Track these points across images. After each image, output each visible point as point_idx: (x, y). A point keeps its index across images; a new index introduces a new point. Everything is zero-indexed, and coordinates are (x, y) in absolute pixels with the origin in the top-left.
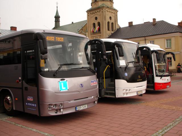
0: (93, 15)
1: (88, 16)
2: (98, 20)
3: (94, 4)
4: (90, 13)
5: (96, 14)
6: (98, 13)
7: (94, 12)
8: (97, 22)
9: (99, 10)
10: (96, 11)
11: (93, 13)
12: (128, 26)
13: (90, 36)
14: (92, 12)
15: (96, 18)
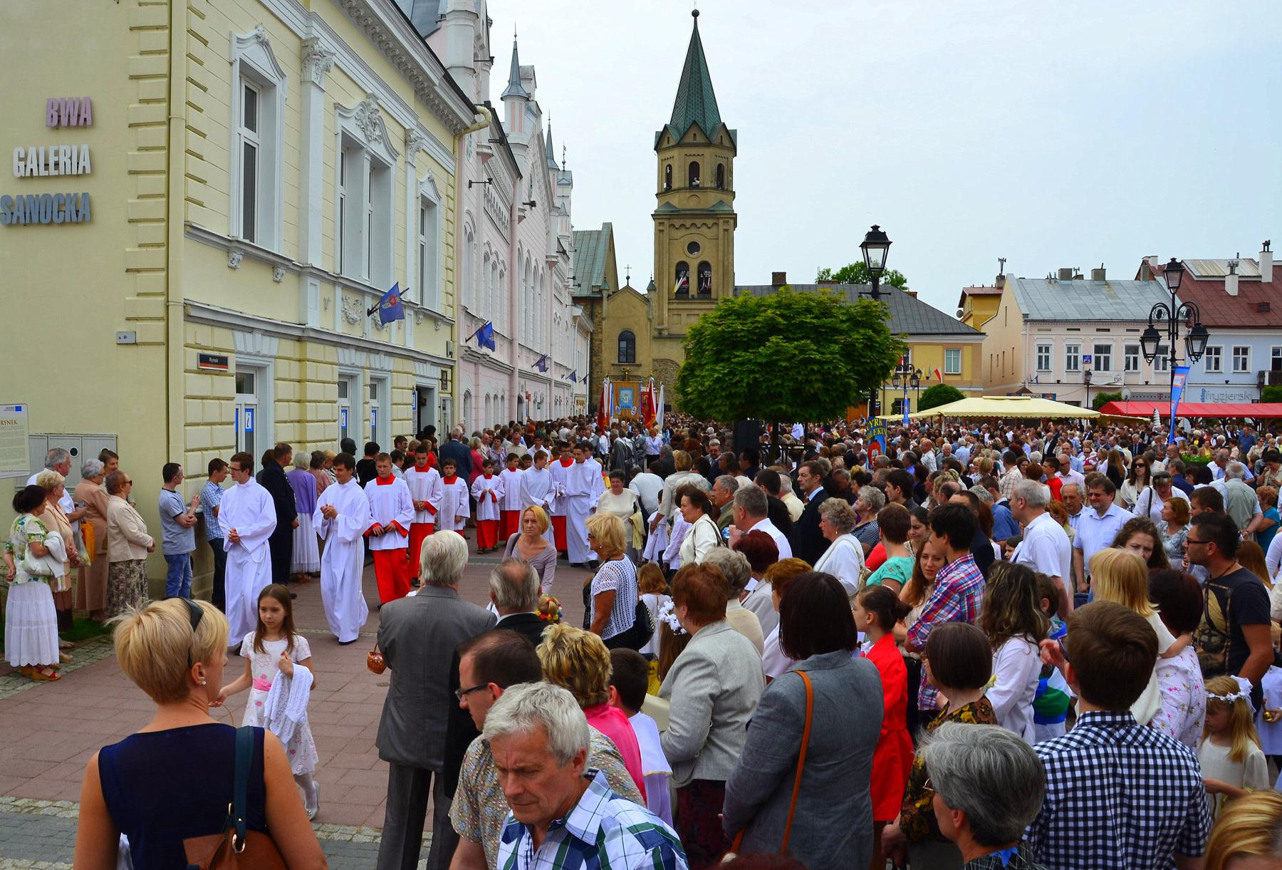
0: (683, 232)
1: (659, 232)
2: (705, 254)
3: (688, 195)
4: (666, 222)
5: (693, 230)
6: (704, 229)
7: (688, 223)
8: (699, 260)
9: (710, 222)
10: (699, 222)
11: (682, 225)
12: (770, 283)
13: (666, 306)
14: (677, 223)
15: (693, 247)
